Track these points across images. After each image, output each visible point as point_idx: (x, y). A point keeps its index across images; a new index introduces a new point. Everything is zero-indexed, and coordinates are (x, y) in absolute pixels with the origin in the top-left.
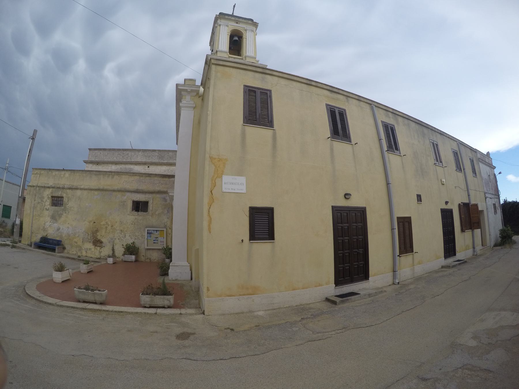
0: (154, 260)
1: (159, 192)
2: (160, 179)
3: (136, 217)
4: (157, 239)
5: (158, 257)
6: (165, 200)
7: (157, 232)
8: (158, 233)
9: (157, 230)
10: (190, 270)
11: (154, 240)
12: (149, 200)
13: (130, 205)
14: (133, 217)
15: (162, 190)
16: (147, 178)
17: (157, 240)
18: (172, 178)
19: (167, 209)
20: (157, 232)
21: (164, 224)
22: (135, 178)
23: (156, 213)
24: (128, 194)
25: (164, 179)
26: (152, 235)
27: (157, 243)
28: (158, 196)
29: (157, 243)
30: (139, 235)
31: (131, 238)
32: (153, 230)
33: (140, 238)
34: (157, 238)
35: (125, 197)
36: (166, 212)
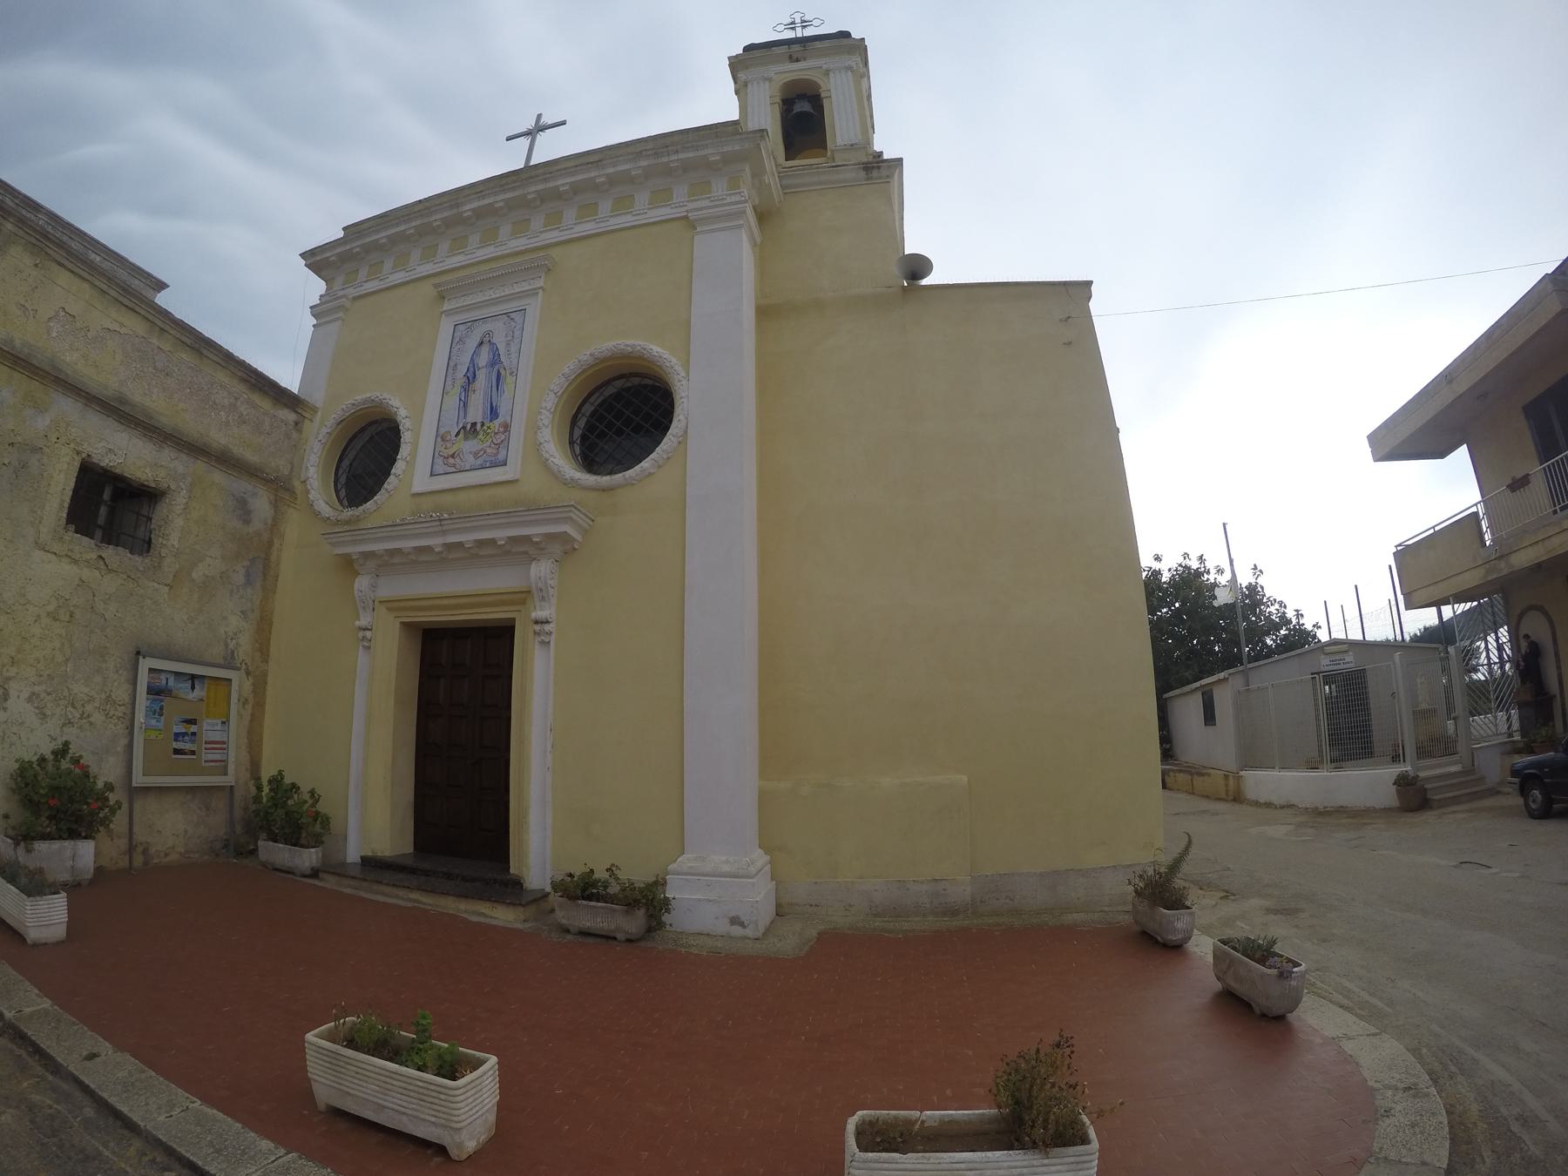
0: (166, 855)
1: (225, 460)
2: (239, 388)
3: (86, 574)
4: (193, 728)
5: (186, 831)
6: (243, 510)
7: (193, 688)
8: (199, 692)
9: (193, 677)
10: (772, 879)
11: (177, 736)
12: (173, 487)
13: (61, 483)
14: (66, 568)
15: (238, 450)
16: (184, 356)
17: (194, 734)
18: (286, 406)
19: (246, 563)
20: (193, 688)
21: (227, 645)
22: (122, 325)
23: (194, 575)
24: (66, 406)
25: (256, 398)
26: (167, 702)
27: (193, 753)
28: (218, 477)
29: (193, 753)
30: (91, 699)
31: (44, 716)
32: (177, 674)
33: (98, 718)
34: (192, 722)
35: (43, 422)
36: (239, 578)
